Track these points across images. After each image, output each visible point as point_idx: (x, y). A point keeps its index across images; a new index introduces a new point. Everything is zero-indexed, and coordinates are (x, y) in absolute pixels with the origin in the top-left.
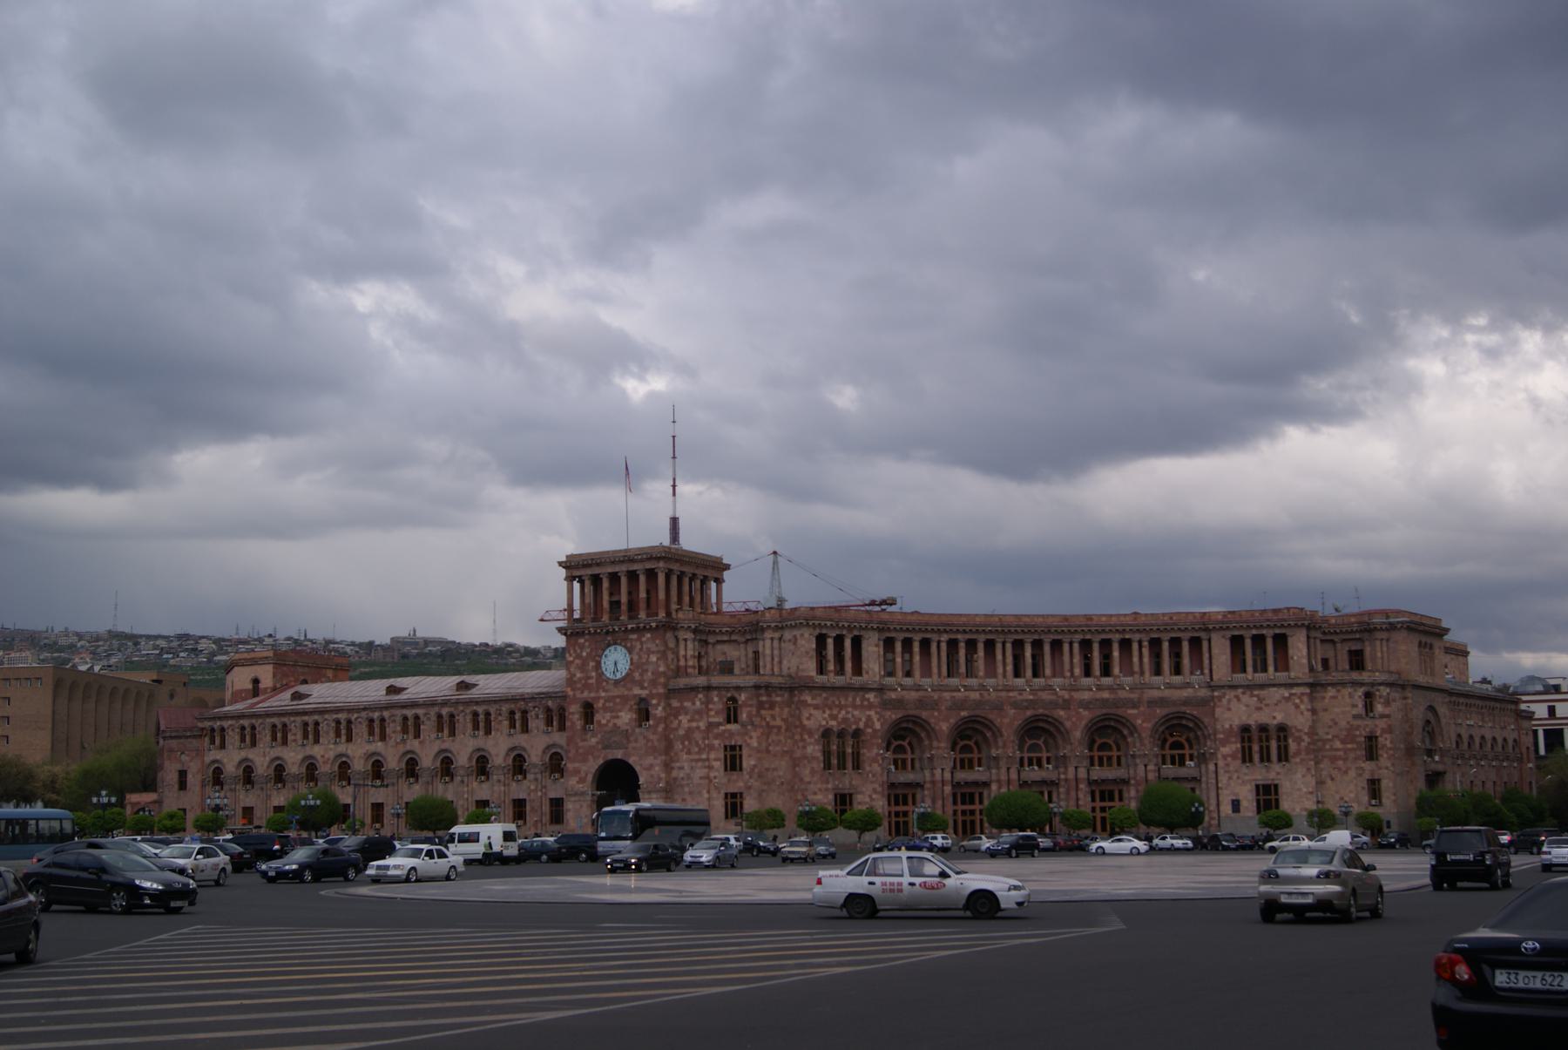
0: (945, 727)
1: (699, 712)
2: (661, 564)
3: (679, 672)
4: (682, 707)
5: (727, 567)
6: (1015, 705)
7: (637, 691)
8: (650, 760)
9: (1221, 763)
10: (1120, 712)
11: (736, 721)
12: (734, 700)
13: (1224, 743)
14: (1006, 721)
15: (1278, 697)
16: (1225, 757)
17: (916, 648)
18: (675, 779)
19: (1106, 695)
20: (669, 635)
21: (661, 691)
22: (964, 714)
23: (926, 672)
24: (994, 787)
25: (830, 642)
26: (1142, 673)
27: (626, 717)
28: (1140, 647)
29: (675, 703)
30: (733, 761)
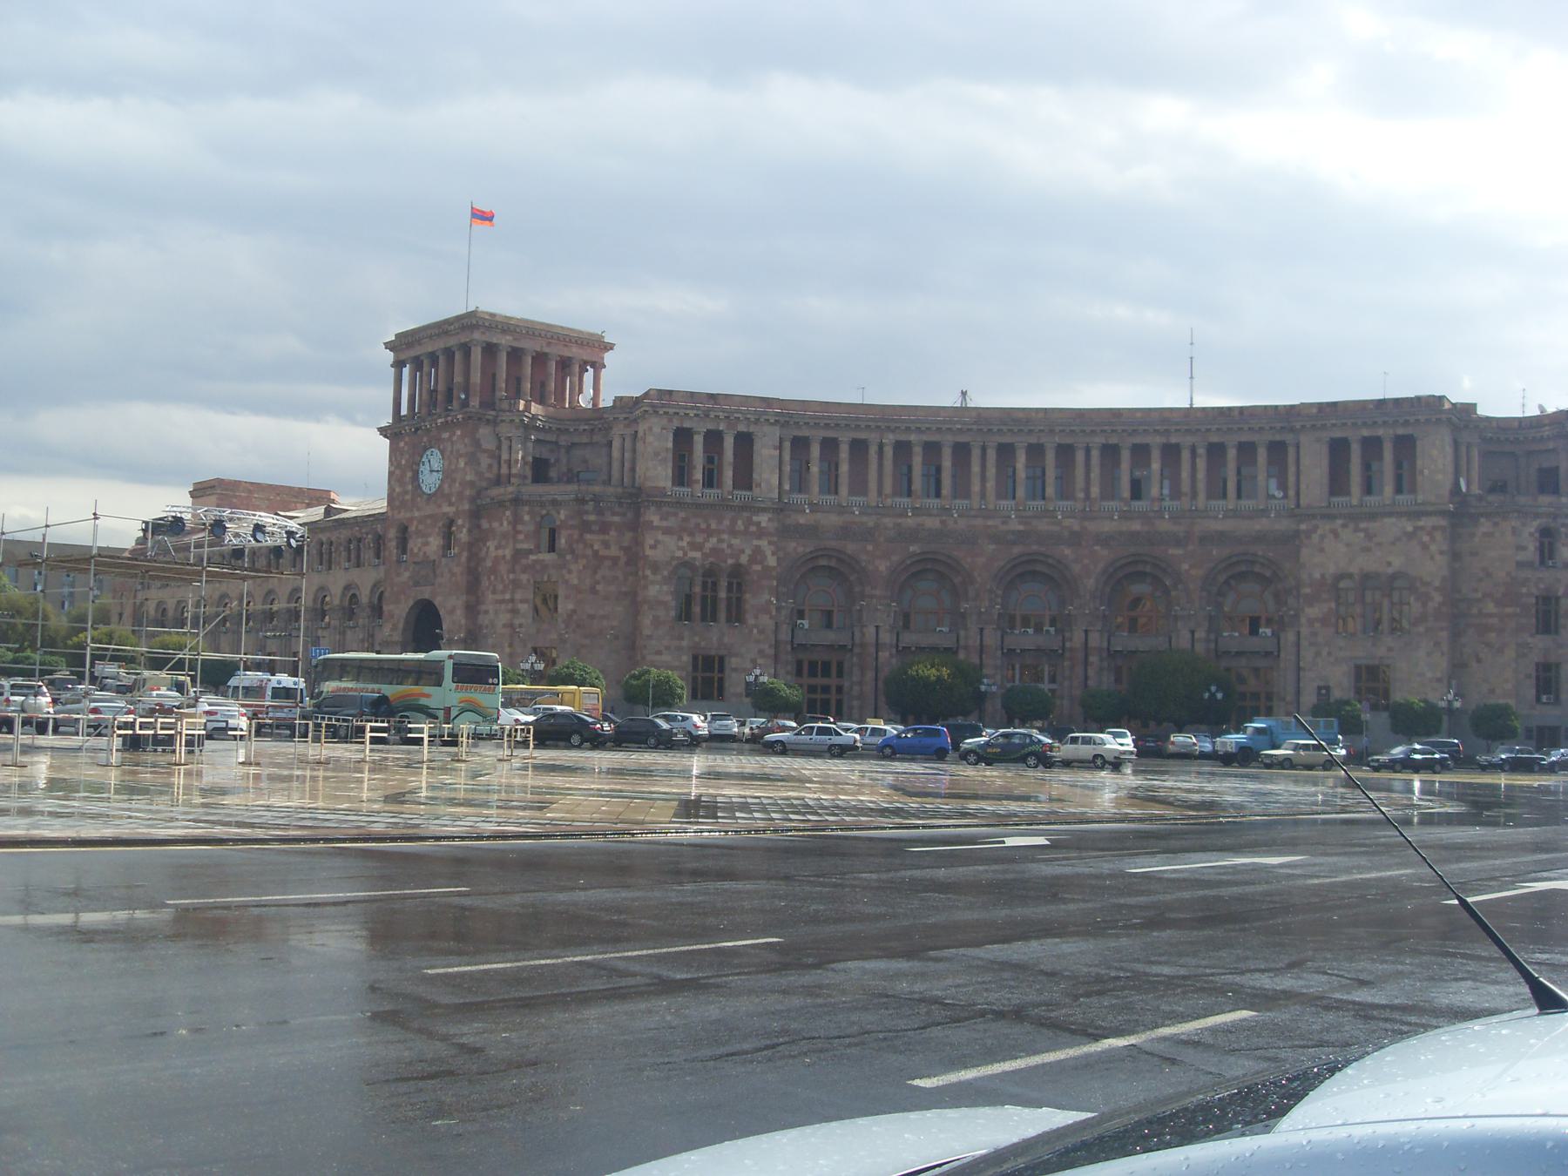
0: (883, 566)
1: (504, 536)
2: (477, 335)
5: (609, 347)
7: (447, 509)
9: (1305, 631)
11: (552, 549)
16: (1311, 622)
17: (844, 453)
19: (1136, 526)
20: (484, 432)
21: (466, 507)
23: (859, 487)
24: (962, 656)
25: (699, 440)
26: (1194, 495)
27: (435, 542)
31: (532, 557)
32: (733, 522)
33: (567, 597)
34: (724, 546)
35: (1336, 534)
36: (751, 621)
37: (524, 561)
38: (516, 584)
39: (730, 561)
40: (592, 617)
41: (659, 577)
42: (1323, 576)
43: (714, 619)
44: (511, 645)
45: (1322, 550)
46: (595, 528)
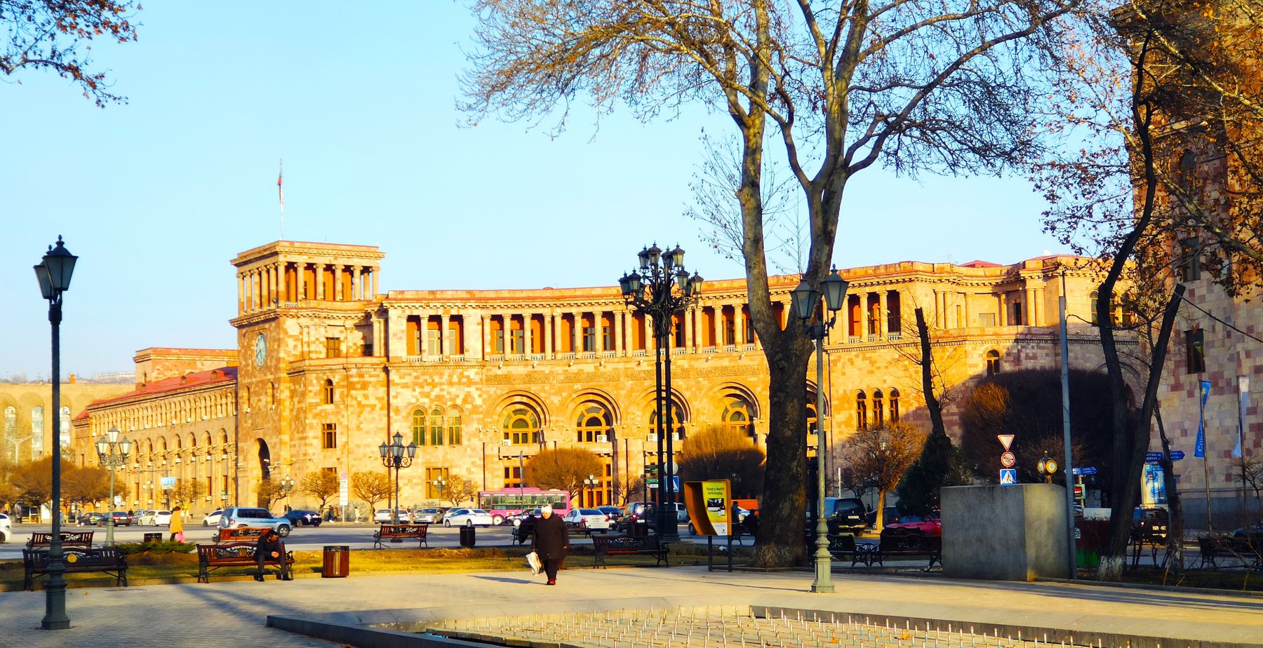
6: (632, 376)
10: (740, 380)
12: (330, 382)
14: (623, 392)
15: (888, 358)
22: (578, 386)
30: (330, 441)
32: (451, 376)
34: (445, 393)
35: (852, 363)
36: (464, 441)
39: (449, 403)
40: (358, 446)
41: (399, 417)
43: (441, 443)
45: (844, 374)
46: (358, 386)
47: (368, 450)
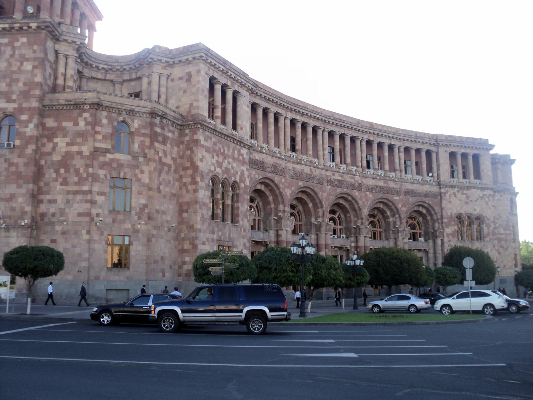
3: (54, 89)
4: (61, 128)
6: (331, 183)
8: (12, 189)
9: (446, 240)
10: (390, 197)
13: (448, 225)
16: (448, 235)
18: (43, 215)
19: (381, 184)
21: (35, 104)
22: (301, 184)
26: (401, 171)
28: (399, 152)
29: (50, 123)
31: (109, 156)
33: (140, 193)
34: (230, 167)
35: (455, 196)
37: (102, 159)
38: (95, 178)
39: (233, 179)
40: (158, 211)
42: (451, 213)
44: (88, 232)
45: (450, 202)
46: (160, 139)
47: (164, 217)
